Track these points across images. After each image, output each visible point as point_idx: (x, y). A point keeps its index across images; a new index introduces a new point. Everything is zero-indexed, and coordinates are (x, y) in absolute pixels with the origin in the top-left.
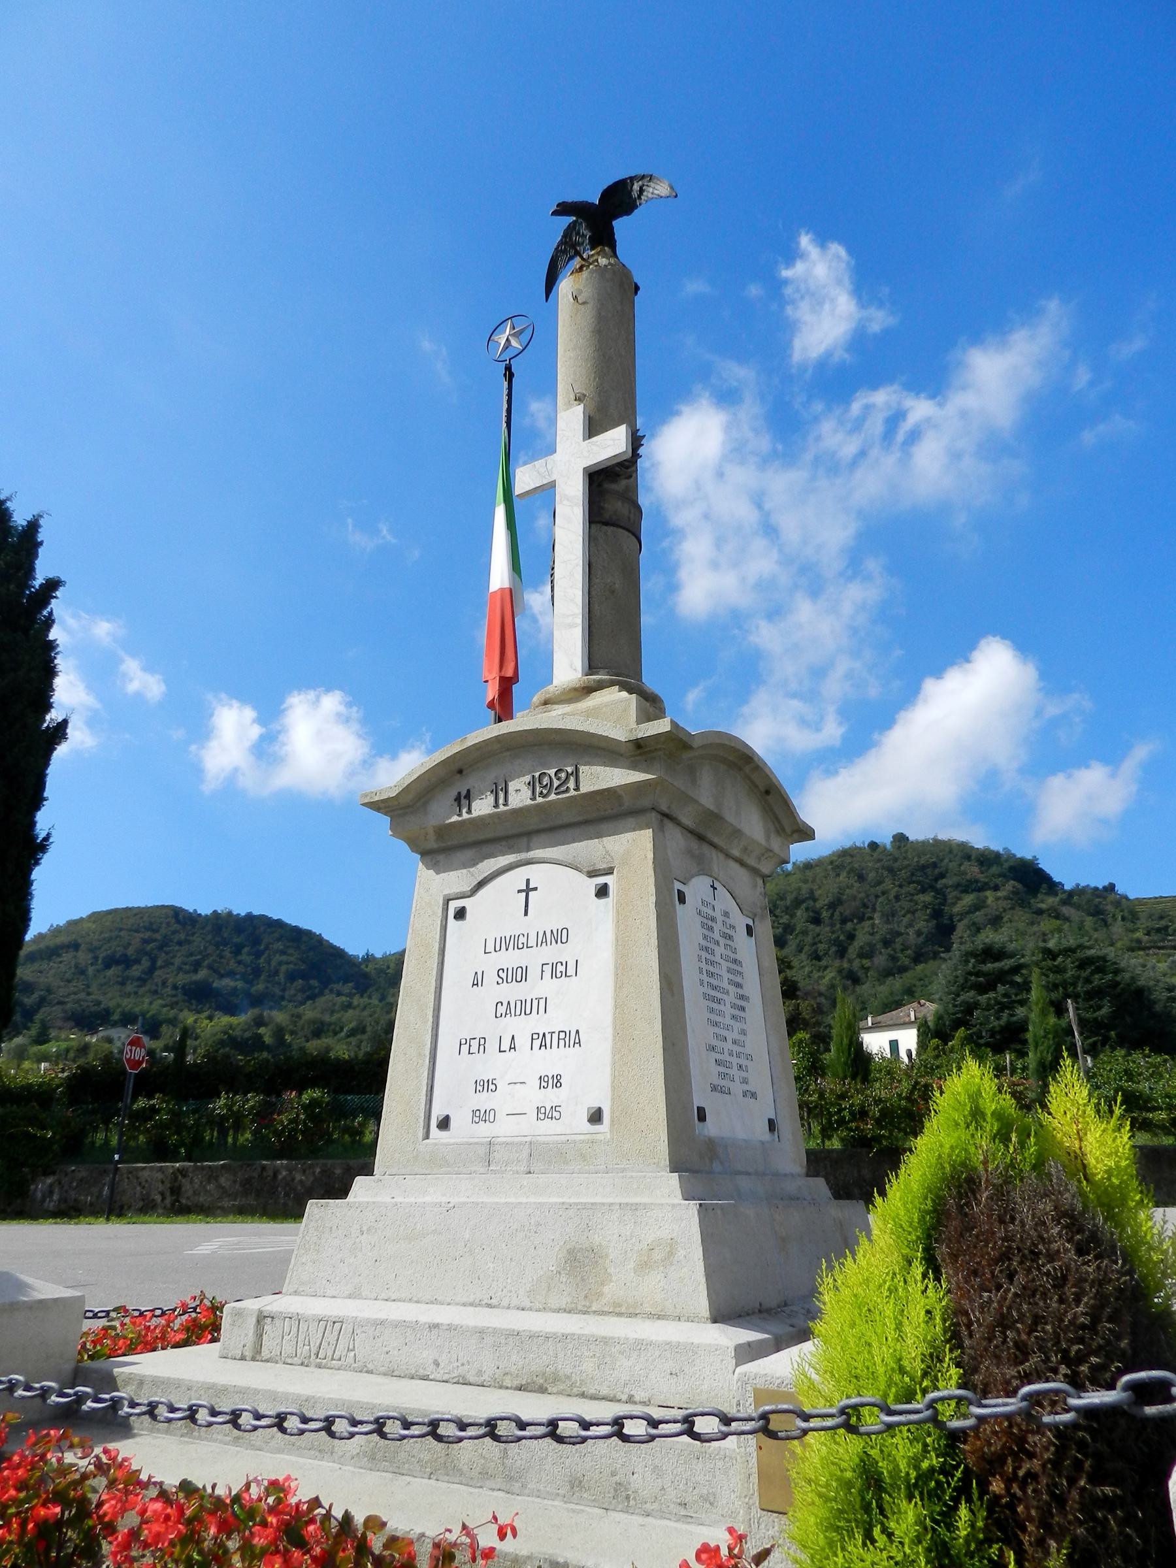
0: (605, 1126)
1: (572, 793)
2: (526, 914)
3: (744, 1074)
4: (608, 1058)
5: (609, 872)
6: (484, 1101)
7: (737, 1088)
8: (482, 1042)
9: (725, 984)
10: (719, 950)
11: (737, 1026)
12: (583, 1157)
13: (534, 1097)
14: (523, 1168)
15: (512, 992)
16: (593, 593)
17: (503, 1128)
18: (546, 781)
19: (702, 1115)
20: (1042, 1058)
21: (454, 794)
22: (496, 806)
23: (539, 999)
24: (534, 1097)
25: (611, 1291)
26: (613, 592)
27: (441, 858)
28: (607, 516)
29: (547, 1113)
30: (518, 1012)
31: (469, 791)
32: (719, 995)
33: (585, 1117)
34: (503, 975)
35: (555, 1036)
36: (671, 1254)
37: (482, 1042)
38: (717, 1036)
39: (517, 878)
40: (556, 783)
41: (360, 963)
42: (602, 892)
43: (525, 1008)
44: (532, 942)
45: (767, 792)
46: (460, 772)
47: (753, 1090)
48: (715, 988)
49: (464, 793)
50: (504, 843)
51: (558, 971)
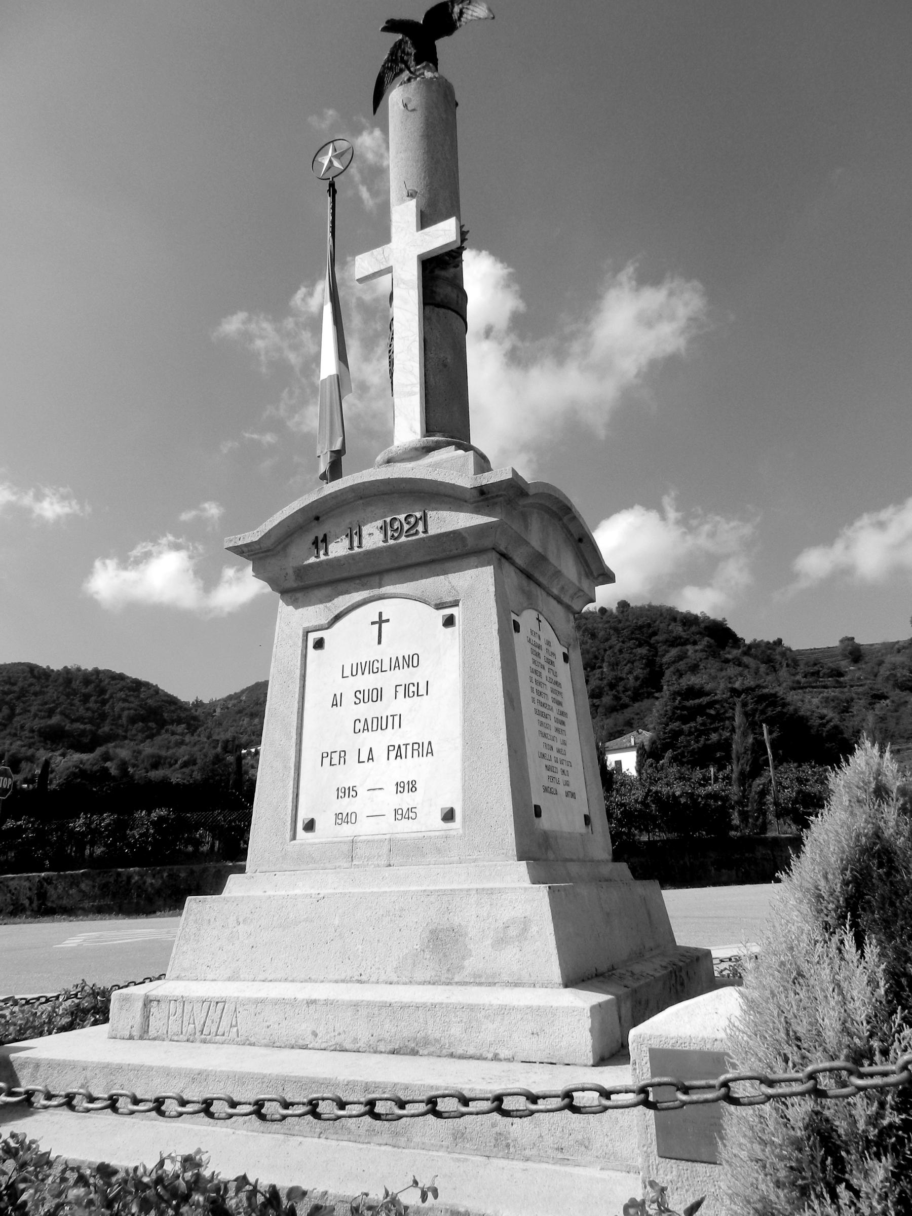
1: (421, 535)
2: (379, 642)
3: (566, 778)
4: (458, 766)
5: (455, 604)
6: (346, 805)
7: (562, 789)
8: (343, 755)
9: (550, 702)
10: (545, 673)
11: (560, 737)
12: (439, 851)
13: (392, 800)
14: (384, 862)
15: (368, 711)
16: (428, 366)
17: (365, 828)
18: (396, 525)
19: (538, 812)
20: (742, 769)
21: (312, 538)
22: (351, 548)
23: (393, 716)
24: (392, 800)
25: (471, 964)
26: (445, 366)
27: (299, 595)
28: (438, 299)
29: (408, 814)
30: (375, 728)
31: (325, 535)
32: (546, 711)
33: (439, 816)
34: (360, 696)
35: (410, 748)
36: (525, 930)
37: (343, 755)
38: (546, 745)
39: (371, 611)
40: (406, 527)
41: (191, 709)
42: (449, 622)
43: (380, 724)
44: (386, 666)
45: (580, 540)
46: (317, 518)
47: (573, 791)
48: (543, 705)
49: (321, 538)
50: (358, 581)
51: (410, 691)
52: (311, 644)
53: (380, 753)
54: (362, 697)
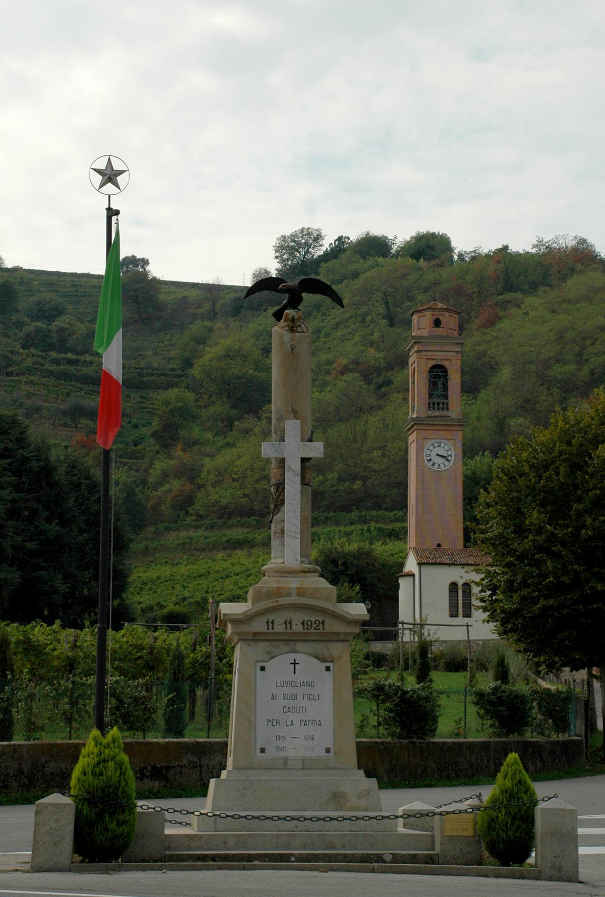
0: (331, 754)
5: (332, 662)
6: (281, 743)
8: (278, 722)
15: (290, 703)
37: (278, 722)
39: (291, 657)
40: (314, 626)
42: (328, 669)
44: (298, 685)
51: (311, 697)
52: (258, 668)
53: (296, 722)
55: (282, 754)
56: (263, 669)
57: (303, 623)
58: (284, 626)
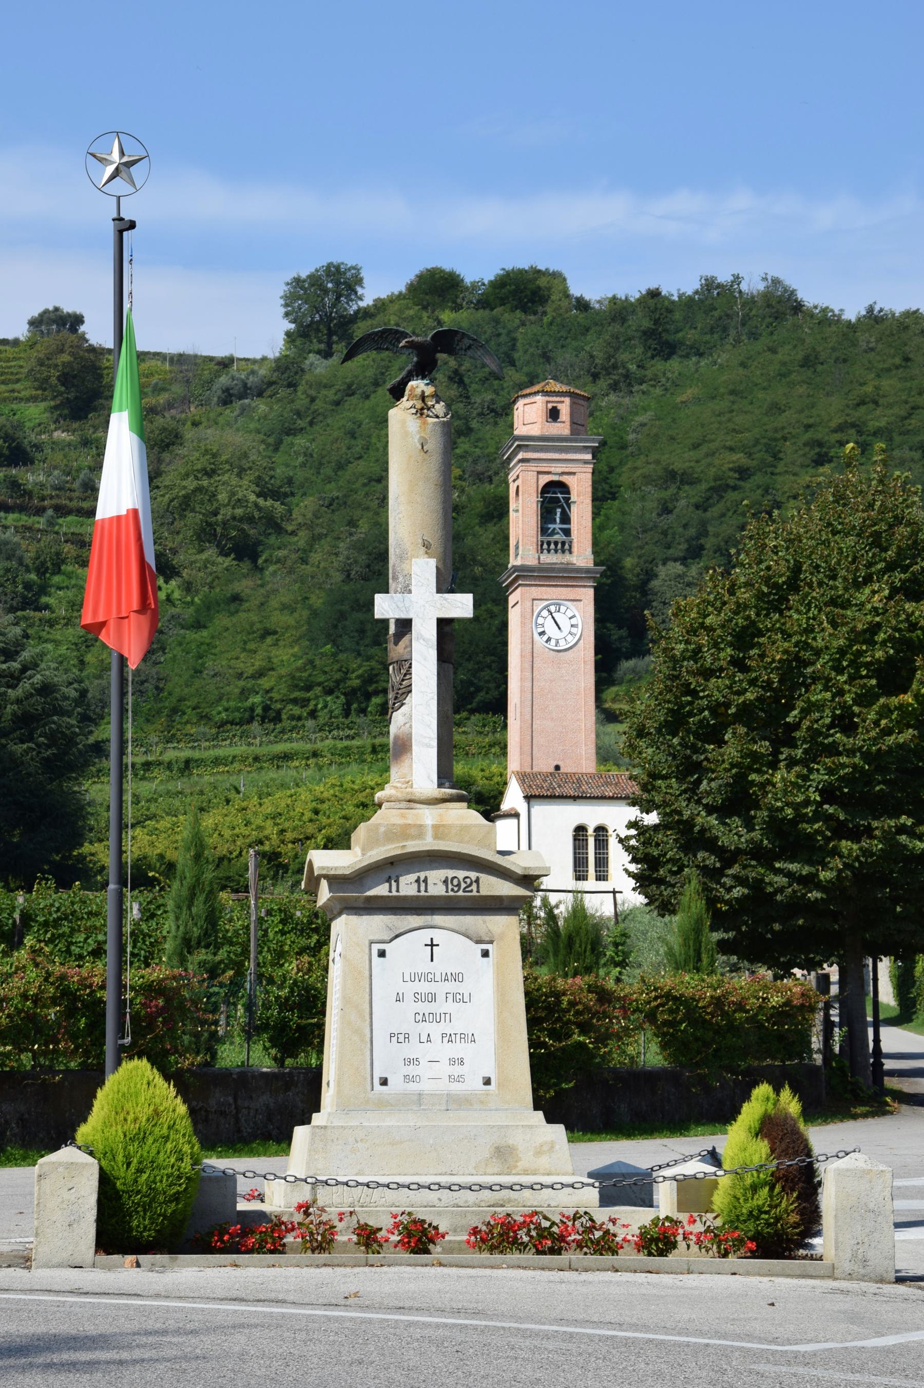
1: (475, 893)
5: (491, 942)
6: (411, 1070)
8: (407, 1037)
12: (482, 1102)
13: (444, 1069)
14: (444, 1108)
18: (455, 882)
21: (387, 876)
22: (419, 891)
24: (444, 1069)
25: (521, 1165)
29: (460, 1079)
33: (481, 1082)
36: (552, 1147)
39: (425, 936)
40: (463, 885)
42: (485, 954)
43: (436, 1018)
44: (438, 978)
46: (392, 863)
51: (457, 998)
52: (375, 953)
53: (436, 1037)
54: (418, 997)
55: (413, 1087)
56: (382, 954)
57: (445, 882)
58: (416, 885)
